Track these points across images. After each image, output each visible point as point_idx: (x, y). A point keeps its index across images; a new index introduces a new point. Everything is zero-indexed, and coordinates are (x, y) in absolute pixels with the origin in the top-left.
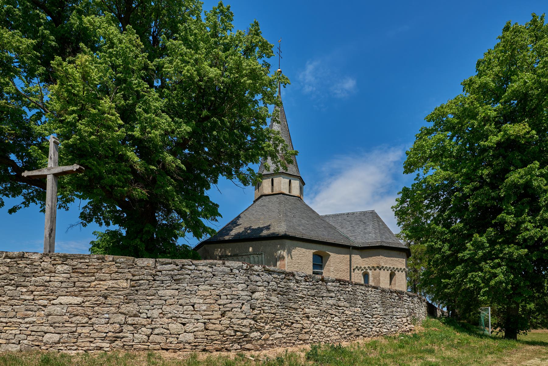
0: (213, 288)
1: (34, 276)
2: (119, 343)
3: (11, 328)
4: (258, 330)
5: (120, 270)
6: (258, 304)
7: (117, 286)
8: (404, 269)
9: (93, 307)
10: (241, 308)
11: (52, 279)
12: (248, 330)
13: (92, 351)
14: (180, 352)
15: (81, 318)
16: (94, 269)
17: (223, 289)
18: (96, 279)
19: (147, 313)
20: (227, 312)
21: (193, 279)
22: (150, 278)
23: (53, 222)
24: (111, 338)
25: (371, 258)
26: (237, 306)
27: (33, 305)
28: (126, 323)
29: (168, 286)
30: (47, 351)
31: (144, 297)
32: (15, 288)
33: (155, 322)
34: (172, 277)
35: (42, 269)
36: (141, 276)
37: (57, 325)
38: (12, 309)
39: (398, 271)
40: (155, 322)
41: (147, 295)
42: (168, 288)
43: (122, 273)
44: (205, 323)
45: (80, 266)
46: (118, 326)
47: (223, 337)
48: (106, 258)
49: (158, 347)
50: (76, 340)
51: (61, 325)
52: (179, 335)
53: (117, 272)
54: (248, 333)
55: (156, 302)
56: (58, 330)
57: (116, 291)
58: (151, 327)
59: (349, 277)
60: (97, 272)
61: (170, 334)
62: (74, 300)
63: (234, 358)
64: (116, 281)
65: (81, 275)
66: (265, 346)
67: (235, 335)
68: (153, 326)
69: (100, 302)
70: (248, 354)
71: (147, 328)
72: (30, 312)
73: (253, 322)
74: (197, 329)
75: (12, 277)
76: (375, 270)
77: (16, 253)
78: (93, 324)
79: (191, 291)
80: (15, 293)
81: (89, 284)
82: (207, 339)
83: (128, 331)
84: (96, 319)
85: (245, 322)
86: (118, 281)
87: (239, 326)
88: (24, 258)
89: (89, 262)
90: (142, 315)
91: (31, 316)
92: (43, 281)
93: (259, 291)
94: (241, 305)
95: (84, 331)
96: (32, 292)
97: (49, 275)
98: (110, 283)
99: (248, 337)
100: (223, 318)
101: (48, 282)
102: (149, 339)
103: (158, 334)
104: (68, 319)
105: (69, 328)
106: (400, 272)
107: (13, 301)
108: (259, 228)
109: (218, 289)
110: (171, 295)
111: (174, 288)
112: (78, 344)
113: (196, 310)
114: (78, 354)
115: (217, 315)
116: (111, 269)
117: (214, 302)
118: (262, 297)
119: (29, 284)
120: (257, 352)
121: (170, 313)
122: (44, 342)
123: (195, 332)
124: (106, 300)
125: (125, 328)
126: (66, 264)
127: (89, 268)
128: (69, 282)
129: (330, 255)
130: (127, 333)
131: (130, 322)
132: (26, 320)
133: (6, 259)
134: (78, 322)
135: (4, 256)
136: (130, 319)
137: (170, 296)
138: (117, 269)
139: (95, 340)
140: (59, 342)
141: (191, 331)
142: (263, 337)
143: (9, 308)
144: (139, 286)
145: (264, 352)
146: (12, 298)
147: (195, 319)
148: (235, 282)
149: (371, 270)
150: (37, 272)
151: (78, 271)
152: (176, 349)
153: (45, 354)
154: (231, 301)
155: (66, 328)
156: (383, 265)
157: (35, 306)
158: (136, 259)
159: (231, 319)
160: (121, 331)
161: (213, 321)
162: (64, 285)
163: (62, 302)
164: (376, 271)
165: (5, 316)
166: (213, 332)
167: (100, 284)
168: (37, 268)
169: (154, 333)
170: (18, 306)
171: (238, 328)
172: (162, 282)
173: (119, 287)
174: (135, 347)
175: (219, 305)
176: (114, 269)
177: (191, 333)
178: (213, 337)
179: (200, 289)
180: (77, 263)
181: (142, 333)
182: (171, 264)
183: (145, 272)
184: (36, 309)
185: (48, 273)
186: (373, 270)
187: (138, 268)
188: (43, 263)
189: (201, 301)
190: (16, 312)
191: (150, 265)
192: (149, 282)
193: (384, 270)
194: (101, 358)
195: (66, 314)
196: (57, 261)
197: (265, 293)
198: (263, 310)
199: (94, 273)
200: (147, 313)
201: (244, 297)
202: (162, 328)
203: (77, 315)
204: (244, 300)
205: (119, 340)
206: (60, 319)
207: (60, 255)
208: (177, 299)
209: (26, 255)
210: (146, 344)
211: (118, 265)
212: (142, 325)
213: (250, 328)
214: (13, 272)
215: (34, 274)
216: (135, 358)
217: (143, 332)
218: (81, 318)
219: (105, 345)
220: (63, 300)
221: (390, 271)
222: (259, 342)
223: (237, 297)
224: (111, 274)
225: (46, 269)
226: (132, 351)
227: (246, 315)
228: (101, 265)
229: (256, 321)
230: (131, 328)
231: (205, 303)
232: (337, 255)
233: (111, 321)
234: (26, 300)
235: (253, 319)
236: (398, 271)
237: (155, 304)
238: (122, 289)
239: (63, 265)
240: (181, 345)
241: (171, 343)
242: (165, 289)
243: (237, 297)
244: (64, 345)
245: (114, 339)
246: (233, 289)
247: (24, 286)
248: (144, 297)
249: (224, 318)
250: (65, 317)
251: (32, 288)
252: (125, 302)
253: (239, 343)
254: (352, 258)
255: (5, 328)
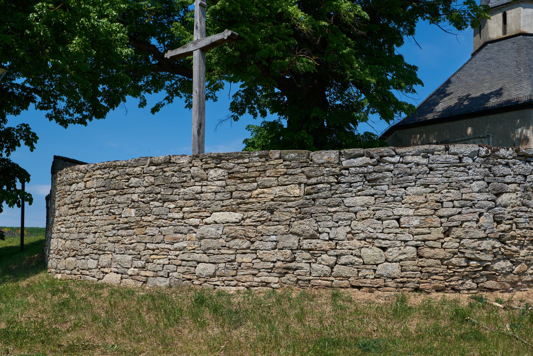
0: (429, 190)
1: (182, 187)
2: (290, 277)
3: (159, 257)
4: (507, 257)
5: (290, 171)
6: (507, 213)
7: (286, 194)
9: (256, 226)
10: (477, 221)
11: (204, 189)
12: (489, 257)
13: (256, 288)
14: (380, 292)
15: (241, 241)
16: (256, 171)
17: (446, 190)
18: (258, 186)
19: (329, 233)
20: (454, 229)
21: (398, 178)
22: (332, 179)
23: (202, 113)
24: (280, 270)
26: (470, 217)
27: (183, 225)
28: (300, 248)
29: (359, 191)
30: (201, 287)
31: (325, 209)
32: (161, 204)
33: (341, 245)
34: (365, 177)
35: (192, 176)
36: (319, 178)
37: (212, 251)
38: (159, 231)
40: (341, 245)
41: (329, 206)
42: (359, 193)
43: (293, 175)
44: (417, 247)
45: (237, 168)
46: (289, 252)
47: (448, 268)
48: (270, 155)
49: (345, 283)
50: (235, 271)
51: (216, 252)
52: (377, 265)
53: (286, 174)
54: (489, 263)
55: (342, 215)
56: (213, 258)
57: (285, 201)
58: (336, 253)
60: (259, 176)
61: (364, 264)
62: (232, 217)
63: (466, 304)
64: (285, 187)
65: (239, 181)
66: (520, 283)
67: (468, 266)
68: (339, 252)
69: (264, 219)
70: (490, 297)
71: (330, 256)
72: (179, 235)
73: (498, 244)
74: (405, 256)
75: (158, 190)
77: (161, 158)
78: (256, 250)
79: (394, 197)
80: (163, 211)
81: (249, 194)
82: (421, 272)
83: (303, 259)
84: (260, 243)
85: (485, 245)
86: (288, 186)
87: (474, 252)
88: (171, 163)
89: (249, 162)
90: (321, 236)
91: (181, 240)
92: (193, 193)
93: (509, 192)
94: (477, 216)
95: (245, 260)
96: (181, 208)
97: (201, 184)
98: (277, 190)
99: (489, 269)
100: (447, 239)
101: (199, 193)
102: (332, 272)
103: (345, 265)
104: (225, 243)
105: (226, 256)
107: (160, 220)
109: (438, 191)
110: (363, 204)
111: (368, 193)
112: (238, 277)
113: (403, 226)
114: (238, 292)
115: (437, 233)
116: (278, 170)
117: (432, 212)
118: (514, 201)
119: (177, 197)
120: (507, 295)
121: (363, 231)
122: (197, 274)
123: (401, 260)
124: (273, 216)
125: (299, 255)
126: (220, 168)
127: (250, 170)
128: (224, 192)
130: (301, 262)
131: (305, 247)
132: (176, 245)
133: (151, 167)
134: (237, 247)
135: (148, 163)
136: (305, 241)
137: (362, 206)
138: (285, 170)
139: (260, 272)
140: (214, 275)
141: (395, 260)
142: (517, 269)
143: (155, 231)
144: (316, 193)
145: (518, 294)
146: (159, 217)
147: (401, 241)
148: (466, 178)
150: (185, 181)
151: (236, 175)
152: (372, 287)
153: (198, 291)
154: (460, 210)
155: (222, 256)
157: (186, 226)
158: (312, 153)
159: (461, 239)
160: (294, 260)
161: (431, 243)
162: (218, 196)
163: (217, 220)
165: (151, 241)
166: (431, 262)
167: (264, 193)
168: (186, 176)
169: (339, 263)
170: (166, 228)
171: (473, 254)
172: (350, 184)
173: (289, 195)
174: (313, 282)
175: (441, 217)
176: (282, 169)
177: (396, 262)
178: (430, 269)
179: (408, 193)
180: (233, 165)
181: (323, 262)
182: (362, 156)
183: (325, 170)
184: (185, 230)
185: (199, 181)
187: (315, 166)
188: (192, 168)
189: (411, 212)
190: (164, 236)
191: (332, 160)
192: (331, 186)
194: (269, 298)
195: (222, 236)
196: (209, 164)
197: (519, 195)
198: (516, 223)
199: (256, 177)
200: (329, 233)
201: (483, 202)
202: (352, 254)
203: (236, 238)
204: (482, 208)
205: (291, 272)
206: (214, 243)
207: (212, 155)
208: (373, 210)
209: (173, 160)
210: (329, 278)
211: (287, 163)
212: (323, 251)
213: (494, 253)
214: (158, 183)
215: (183, 184)
216: (315, 299)
217: (323, 260)
218: (241, 241)
219: (273, 279)
220: (218, 217)
222: (509, 277)
223: (469, 203)
224: (278, 177)
225: (197, 176)
226: (308, 288)
227: (487, 232)
228: (264, 165)
229: (503, 243)
230: (307, 255)
231: (418, 215)
233: (280, 246)
234: (174, 219)
235: (499, 239)
237: (340, 220)
238: (293, 199)
239: (217, 169)
240: (381, 282)
241: (365, 278)
242: (354, 195)
243: (469, 203)
244: (221, 278)
245: (285, 271)
246: (463, 190)
247: (173, 201)
248: (325, 209)
249: (450, 238)
250: (221, 240)
251: (181, 203)
252: (298, 218)
253: (473, 279)
255: (152, 257)
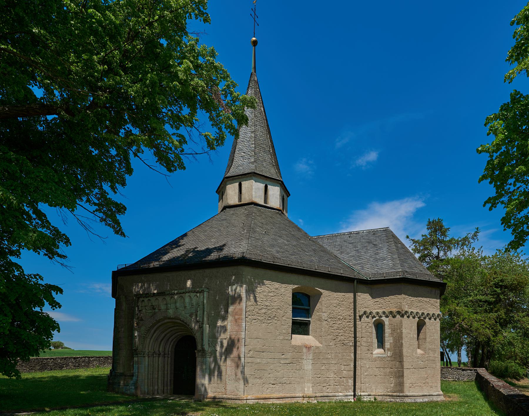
8: (439, 315)
25: (387, 299)
39: (430, 319)
76: (394, 317)
106: (433, 319)
108: (207, 249)
129: (321, 294)
156: (406, 309)
164: (396, 319)
186: (391, 317)
193: (408, 317)
221: (417, 319)
232: (333, 293)
236: (430, 319)
254: (358, 298)
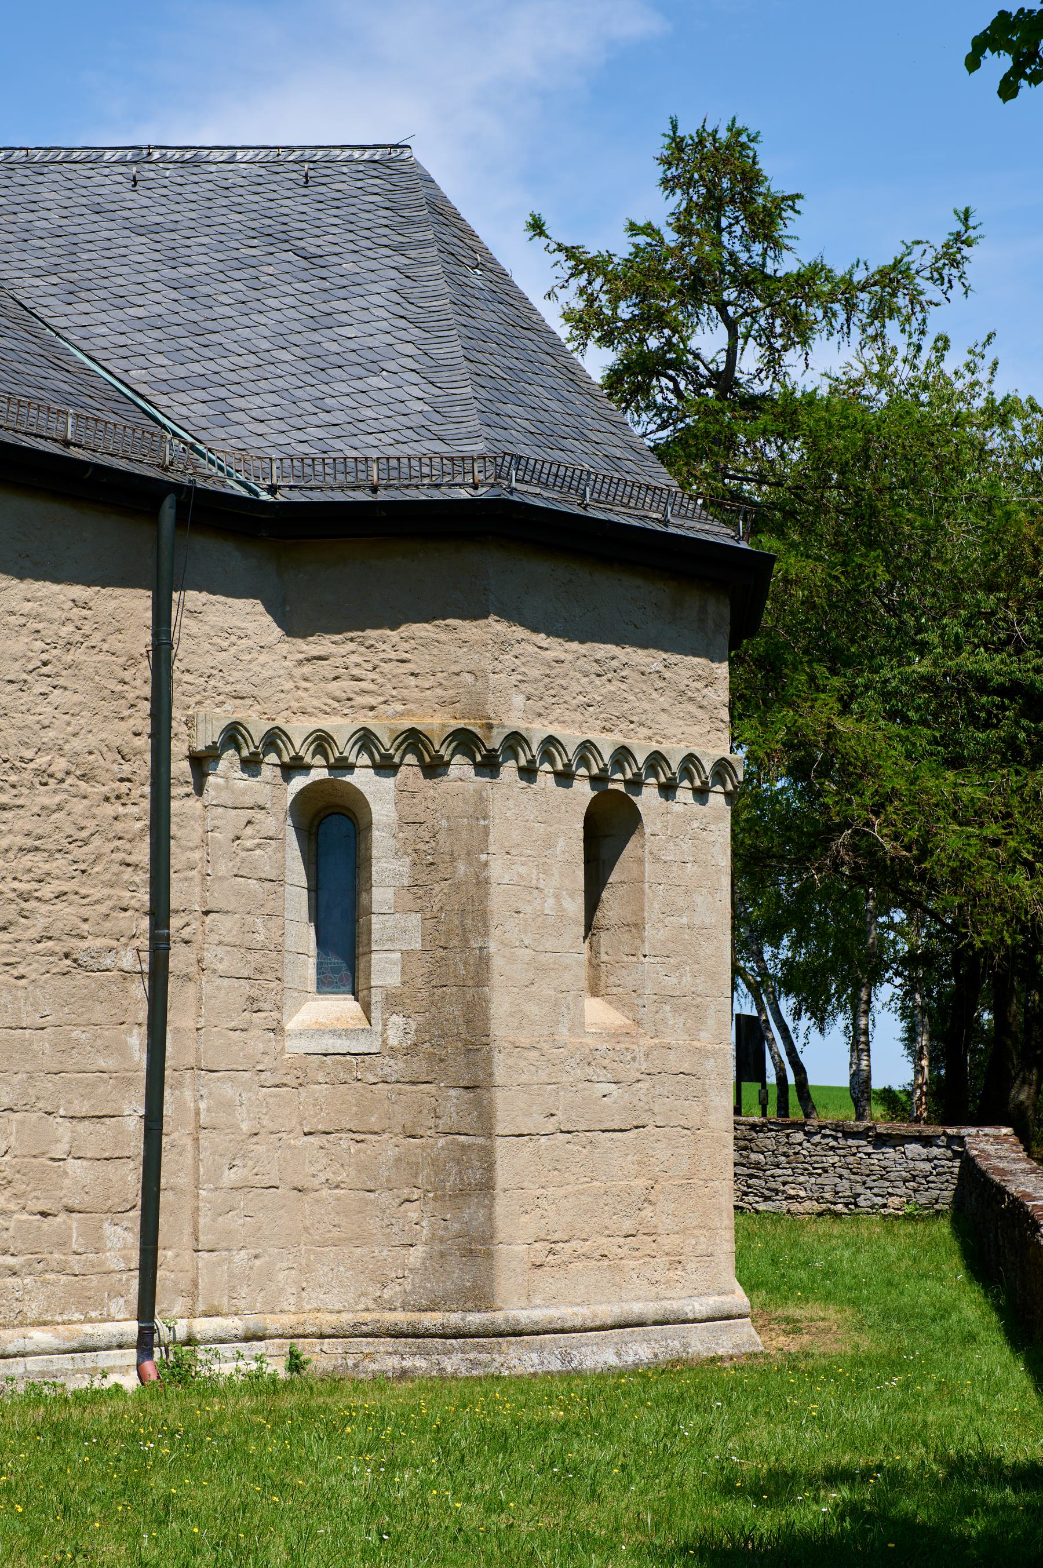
8: (722, 767)
39: (668, 790)
59: (142, 853)
76: (434, 768)
149: (385, 767)
156: (514, 722)
186: (410, 771)
193: (528, 773)
221: (583, 792)
236: (668, 790)
